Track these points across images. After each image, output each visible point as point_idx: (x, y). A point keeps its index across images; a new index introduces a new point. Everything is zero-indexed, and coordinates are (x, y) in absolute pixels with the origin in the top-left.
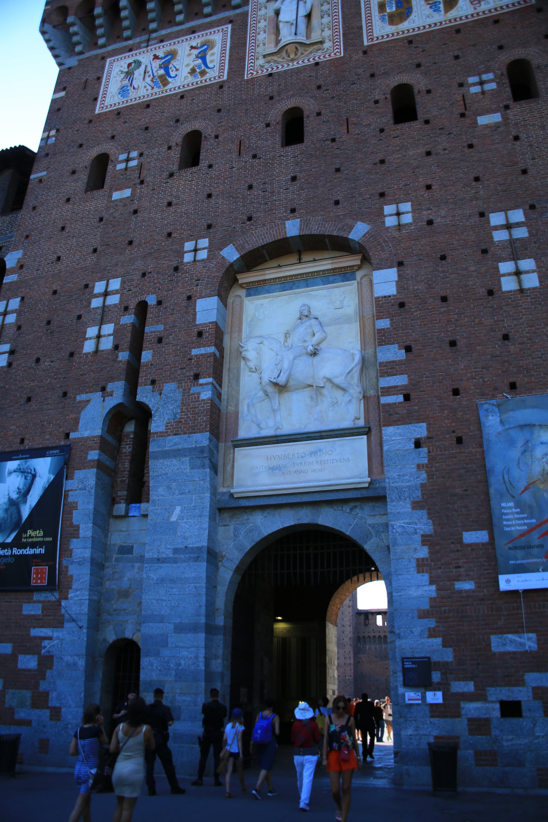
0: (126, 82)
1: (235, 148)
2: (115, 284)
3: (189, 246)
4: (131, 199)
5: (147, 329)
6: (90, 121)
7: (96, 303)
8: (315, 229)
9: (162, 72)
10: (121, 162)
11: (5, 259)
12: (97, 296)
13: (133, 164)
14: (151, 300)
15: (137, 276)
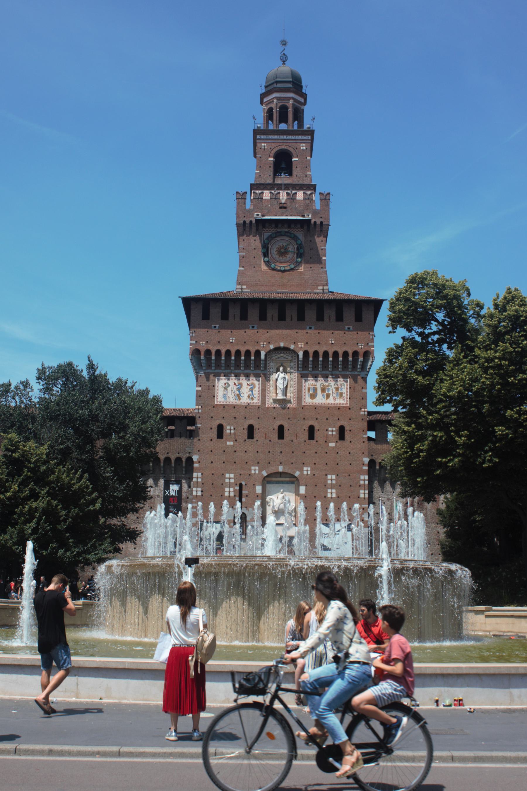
0: (225, 392)
1: (264, 435)
2: (232, 476)
3: (253, 468)
4: (233, 446)
5: (243, 492)
6: (214, 407)
7: (227, 481)
8: (286, 471)
9: (238, 392)
10: (228, 429)
11: (193, 457)
12: (227, 478)
13: (232, 431)
14: (243, 483)
15: (238, 475)
